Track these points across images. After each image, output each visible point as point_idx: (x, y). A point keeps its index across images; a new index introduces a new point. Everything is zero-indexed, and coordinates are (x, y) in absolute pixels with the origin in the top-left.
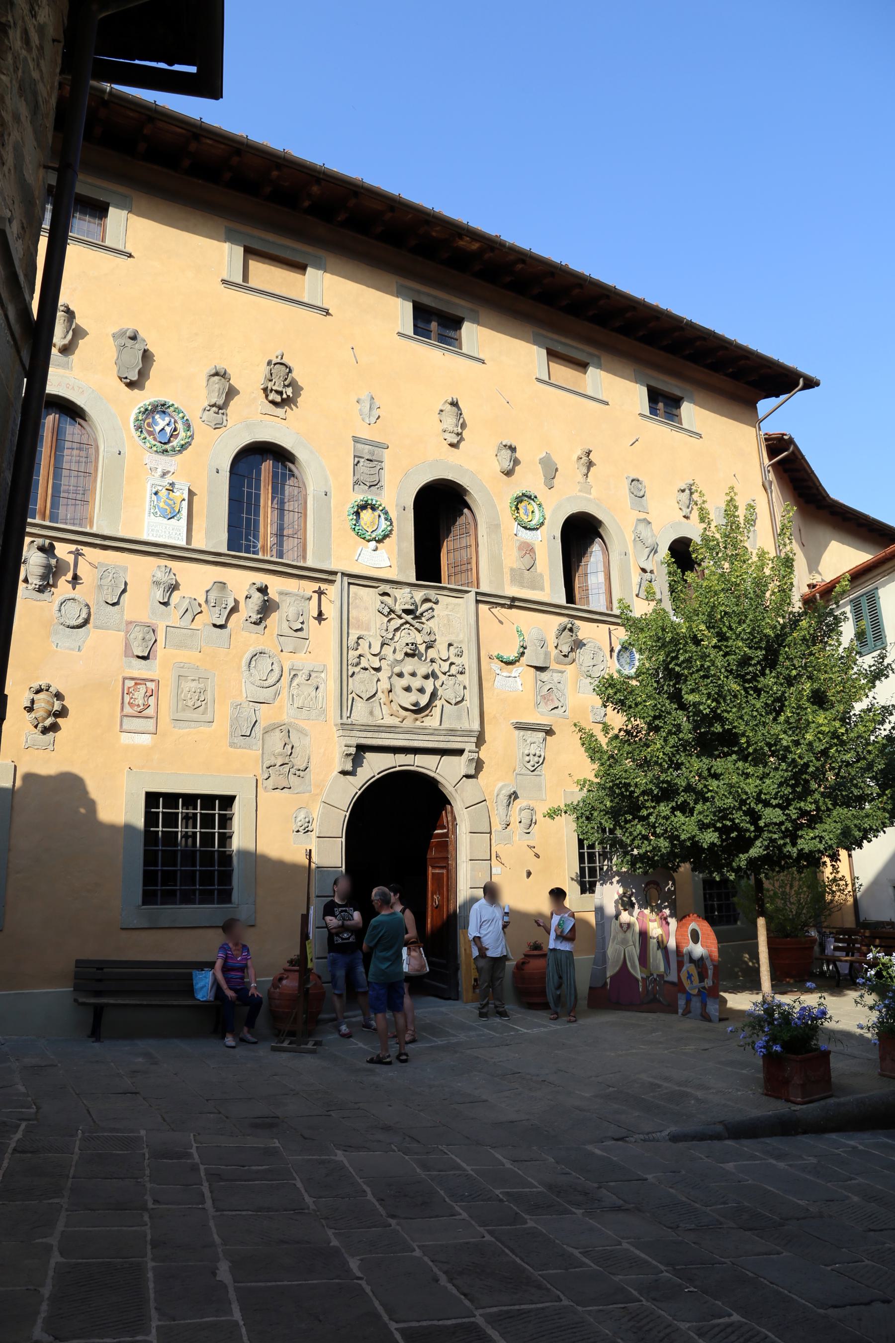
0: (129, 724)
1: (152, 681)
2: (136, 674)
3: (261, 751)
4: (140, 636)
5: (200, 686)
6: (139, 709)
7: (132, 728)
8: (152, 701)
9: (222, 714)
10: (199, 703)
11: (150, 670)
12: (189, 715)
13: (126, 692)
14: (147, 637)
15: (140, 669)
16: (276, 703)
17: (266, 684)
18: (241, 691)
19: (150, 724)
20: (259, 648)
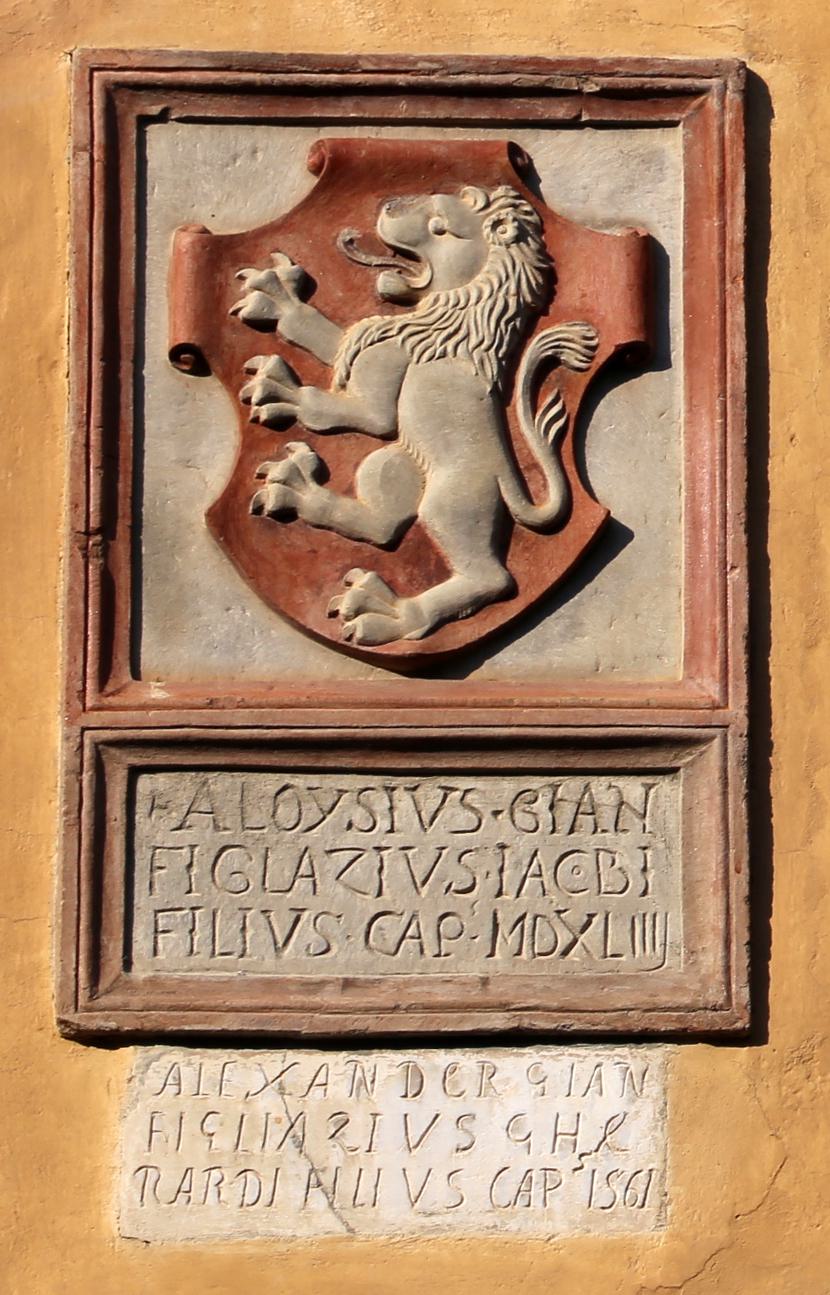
0: (230, 890)
1: (634, 99)
6: (409, 616)
7: (320, 957)
8: (651, 455)
13: (164, 325)
19: (644, 868)
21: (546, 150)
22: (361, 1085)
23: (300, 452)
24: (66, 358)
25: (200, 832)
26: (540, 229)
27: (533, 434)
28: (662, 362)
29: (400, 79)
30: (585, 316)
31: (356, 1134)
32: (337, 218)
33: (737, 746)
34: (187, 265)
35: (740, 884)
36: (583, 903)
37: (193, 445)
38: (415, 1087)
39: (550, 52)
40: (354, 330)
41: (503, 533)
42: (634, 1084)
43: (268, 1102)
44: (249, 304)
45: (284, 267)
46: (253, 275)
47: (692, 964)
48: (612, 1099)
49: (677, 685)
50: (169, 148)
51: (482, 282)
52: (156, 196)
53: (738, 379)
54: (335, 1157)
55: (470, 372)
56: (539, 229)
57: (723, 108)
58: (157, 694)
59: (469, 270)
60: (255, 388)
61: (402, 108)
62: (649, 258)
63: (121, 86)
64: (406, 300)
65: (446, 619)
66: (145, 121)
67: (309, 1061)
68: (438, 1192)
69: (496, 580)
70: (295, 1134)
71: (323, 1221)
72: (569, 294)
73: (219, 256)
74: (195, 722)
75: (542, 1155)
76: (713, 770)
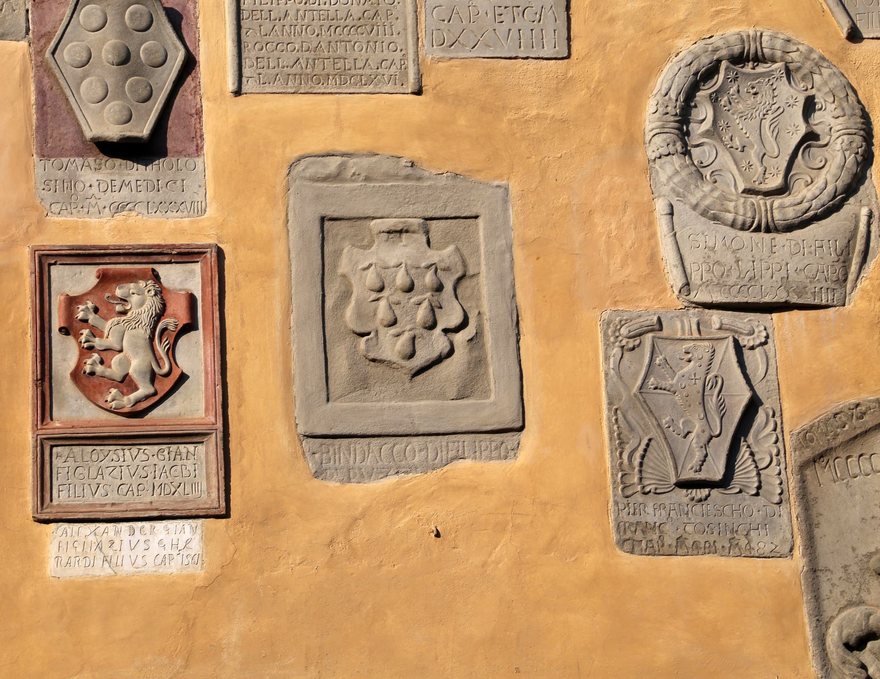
0: (82, 478)
1: (186, 255)
2: (102, 231)
3: (799, 560)
4: (106, 46)
5: (434, 256)
6: (127, 401)
7: (105, 496)
8: (194, 354)
9: (568, 384)
10: (438, 342)
11: (166, 206)
12: (388, 406)
13: (57, 322)
14: (144, 50)
15: (115, 210)
16: (857, 302)
17: (784, 208)
18: (653, 259)
20: (729, 34)
21: (163, 270)
22: (117, 533)
23: (96, 356)
24: (30, 331)
25: (71, 463)
26: (161, 292)
27: (161, 350)
28: (197, 329)
29: (121, 251)
30: (174, 316)
31: (116, 546)
32: (105, 290)
33: (220, 435)
34: (63, 305)
35: (222, 474)
36: (177, 481)
37: (66, 355)
38: (132, 532)
39: (162, 243)
40: (110, 322)
41: (153, 377)
42: (194, 530)
43: (92, 538)
44: (80, 315)
45: (90, 305)
46: (81, 307)
47: (211, 498)
48: (188, 535)
49: (203, 419)
50: (57, 272)
51: (145, 307)
52: (53, 286)
53: (217, 332)
54: (111, 553)
55: (143, 332)
56: (161, 292)
57: (211, 257)
58: (58, 425)
59: (142, 304)
60: (83, 338)
61: (122, 259)
62: (192, 300)
63: (43, 255)
64: (124, 313)
65: (138, 402)
66: (50, 265)
67: (102, 526)
68: (140, 562)
69: (151, 390)
70: (99, 547)
71: (108, 571)
72: (170, 310)
73: (72, 302)
74: (69, 432)
75: (168, 551)
76: (213, 442)
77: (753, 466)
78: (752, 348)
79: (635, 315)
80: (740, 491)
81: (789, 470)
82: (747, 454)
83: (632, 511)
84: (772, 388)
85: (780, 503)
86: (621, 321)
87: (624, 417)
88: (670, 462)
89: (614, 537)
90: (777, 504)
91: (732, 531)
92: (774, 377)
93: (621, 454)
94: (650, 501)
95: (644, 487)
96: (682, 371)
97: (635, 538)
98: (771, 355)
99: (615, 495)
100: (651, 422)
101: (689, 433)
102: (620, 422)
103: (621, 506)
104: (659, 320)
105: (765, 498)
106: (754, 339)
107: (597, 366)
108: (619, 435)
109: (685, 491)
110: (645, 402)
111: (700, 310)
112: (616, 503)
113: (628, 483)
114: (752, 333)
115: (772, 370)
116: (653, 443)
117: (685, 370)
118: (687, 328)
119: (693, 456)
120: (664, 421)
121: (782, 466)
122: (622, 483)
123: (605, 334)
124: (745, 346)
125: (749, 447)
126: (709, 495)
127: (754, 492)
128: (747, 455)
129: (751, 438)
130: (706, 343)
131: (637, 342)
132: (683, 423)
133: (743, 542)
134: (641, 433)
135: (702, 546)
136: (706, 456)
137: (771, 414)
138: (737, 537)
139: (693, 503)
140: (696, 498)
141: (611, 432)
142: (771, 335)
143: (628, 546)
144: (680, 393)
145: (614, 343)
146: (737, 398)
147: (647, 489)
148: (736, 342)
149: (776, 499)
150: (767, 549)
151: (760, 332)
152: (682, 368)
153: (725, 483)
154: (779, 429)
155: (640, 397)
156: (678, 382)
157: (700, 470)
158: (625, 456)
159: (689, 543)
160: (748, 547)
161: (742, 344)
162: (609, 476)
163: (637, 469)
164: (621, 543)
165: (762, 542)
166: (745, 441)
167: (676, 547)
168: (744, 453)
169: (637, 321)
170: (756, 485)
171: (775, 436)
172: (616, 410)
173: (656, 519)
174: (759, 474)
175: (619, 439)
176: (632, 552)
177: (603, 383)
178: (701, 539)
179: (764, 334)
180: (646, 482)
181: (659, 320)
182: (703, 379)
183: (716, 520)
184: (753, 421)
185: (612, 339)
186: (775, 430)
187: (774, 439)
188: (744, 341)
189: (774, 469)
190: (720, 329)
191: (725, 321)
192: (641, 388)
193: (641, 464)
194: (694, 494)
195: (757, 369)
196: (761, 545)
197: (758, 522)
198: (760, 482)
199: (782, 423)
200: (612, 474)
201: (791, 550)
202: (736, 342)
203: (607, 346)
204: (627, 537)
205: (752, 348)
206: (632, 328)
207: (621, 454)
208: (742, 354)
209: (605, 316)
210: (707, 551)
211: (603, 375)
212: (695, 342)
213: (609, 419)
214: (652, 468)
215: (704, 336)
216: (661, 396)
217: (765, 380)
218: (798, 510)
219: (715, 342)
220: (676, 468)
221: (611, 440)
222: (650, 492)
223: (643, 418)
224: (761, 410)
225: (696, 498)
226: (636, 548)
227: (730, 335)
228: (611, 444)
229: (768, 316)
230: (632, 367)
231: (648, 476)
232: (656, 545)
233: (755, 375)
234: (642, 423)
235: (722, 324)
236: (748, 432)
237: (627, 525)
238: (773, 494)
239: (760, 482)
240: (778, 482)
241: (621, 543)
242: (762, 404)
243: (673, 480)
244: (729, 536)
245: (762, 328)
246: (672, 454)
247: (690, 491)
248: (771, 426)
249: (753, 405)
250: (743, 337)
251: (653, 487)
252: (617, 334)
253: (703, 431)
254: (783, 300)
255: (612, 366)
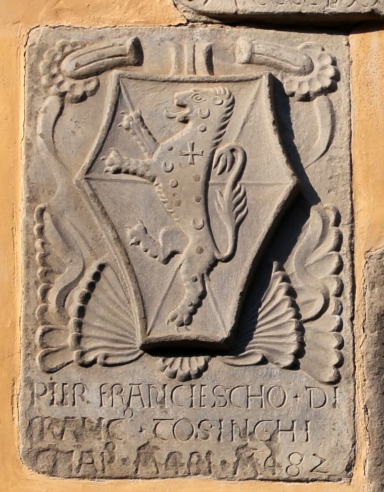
77: (291, 314)
78: (307, 98)
79: (91, 35)
80: (264, 361)
81: (358, 322)
82: (283, 291)
83: (58, 397)
84: (339, 171)
85: (336, 381)
86: (63, 47)
87: (56, 224)
88: (135, 307)
89: (20, 444)
90: (330, 383)
91: (243, 434)
92: (344, 152)
93: (45, 292)
94: (94, 379)
95: (82, 354)
96: (169, 142)
97: (60, 447)
98: (341, 111)
99: (28, 369)
100: (107, 235)
101: (174, 253)
102: (47, 234)
103: (39, 389)
104: (137, 46)
105: (310, 372)
106: (310, 81)
107: (13, 130)
108: (44, 257)
109: (160, 359)
110: (95, 196)
111: (217, 27)
112: (29, 383)
113: (55, 345)
114: (308, 69)
115: (340, 139)
116: (107, 272)
117: (176, 137)
118: (187, 59)
119: (178, 295)
120: (129, 232)
121: (346, 315)
122: (43, 345)
123: (31, 72)
124: (293, 94)
125: (286, 279)
126: (206, 367)
127: (289, 361)
128: (281, 294)
129: (291, 265)
130: (219, 88)
131: (92, 85)
132: (165, 235)
133: (262, 453)
134: (87, 253)
135: (185, 460)
136: (203, 295)
137: (332, 218)
138: (251, 444)
139: (175, 382)
140: (180, 373)
141: (29, 253)
142: (343, 75)
143: (44, 462)
144: (164, 180)
145: (47, 87)
146: (270, 190)
147: (90, 358)
148: (276, 87)
149: (330, 374)
150: (304, 470)
151: (323, 68)
152: (171, 134)
153: (235, 344)
154: (345, 248)
155: (86, 187)
156: (159, 159)
157: (190, 321)
158: (52, 296)
159: (161, 455)
160: (270, 462)
161: (287, 90)
162: (20, 333)
163: (73, 319)
164: (33, 456)
165: (296, 453)
166: (281, 268)
167: (136, 463)
168: (276, 288)
169: (96, 46)
170: (294, 348)
171: (336, 260)
172: (42, 211)
173: (101, 412)
174: (300, 330)
175: (44, 264)
176: (52, 472)
177: (22, 162)
178: (184, 448)
179: (331, 72)
180: (87, 345)
181: (137, 46)
182: (207, 154)
183: (217, 413)
184: (298, 231)
185: (44, 80)
186: (337, 248)
187: (334, 265)
188: (293, 85)
189: (330, 320)
190: (249, 62)
191: (260, 48)
192: (88, 171)
193: (81, 312)
194: (177, 366)
195: (312, 137)
196: (295, 459)
197: (292, 416)
198: (302, 344)
199: (352, 236)
200: (26, 330)
201: (350, 467)
202: (276, 87)
203: (34, 92)
204: (44, 445)
205: (307, 98)
206: (83, 60)
207: (45, 292)
208: (287, 109)
209: (35, 37)
210: (193, 469)
211: (22, 146)
212: (198, 87)
213: (27, 228)
214: (103, 319)
215: (219, 75)
216: (128, 186)
217: (326, 157)
218: (369, 394)
219: (235, 87)
220: (144, 318)
221: (27, 266)
222: (94, 362)
223: (92, 227)
224: (314, 212)
225: (180, 373)
226: (60, 466)
227: (264, 74)
228: (27, 274)
229: (342, 39)
230: (79, 132)
231: (93, 333)
232: (98, 460)
233: (309, 148)
234: (89, 236)
235: (252, 53)
236: (288, 252)
237: (47, 423)
238: (323, 366)
239: (302, 344)
240: (336, 343)
241: (33, 456)
242: (317, 200)
243: (139, 341)
244: (237, 442)
245: (328, 61)
246: (139, 292)
247: (170, 360)
248: (331, 241)
249: (300, 202)
250: (292, 77)
251: (100, 353)
252: (55, 70)
253: (201, 251)
254: (367, 9)
255: (39, 130)
